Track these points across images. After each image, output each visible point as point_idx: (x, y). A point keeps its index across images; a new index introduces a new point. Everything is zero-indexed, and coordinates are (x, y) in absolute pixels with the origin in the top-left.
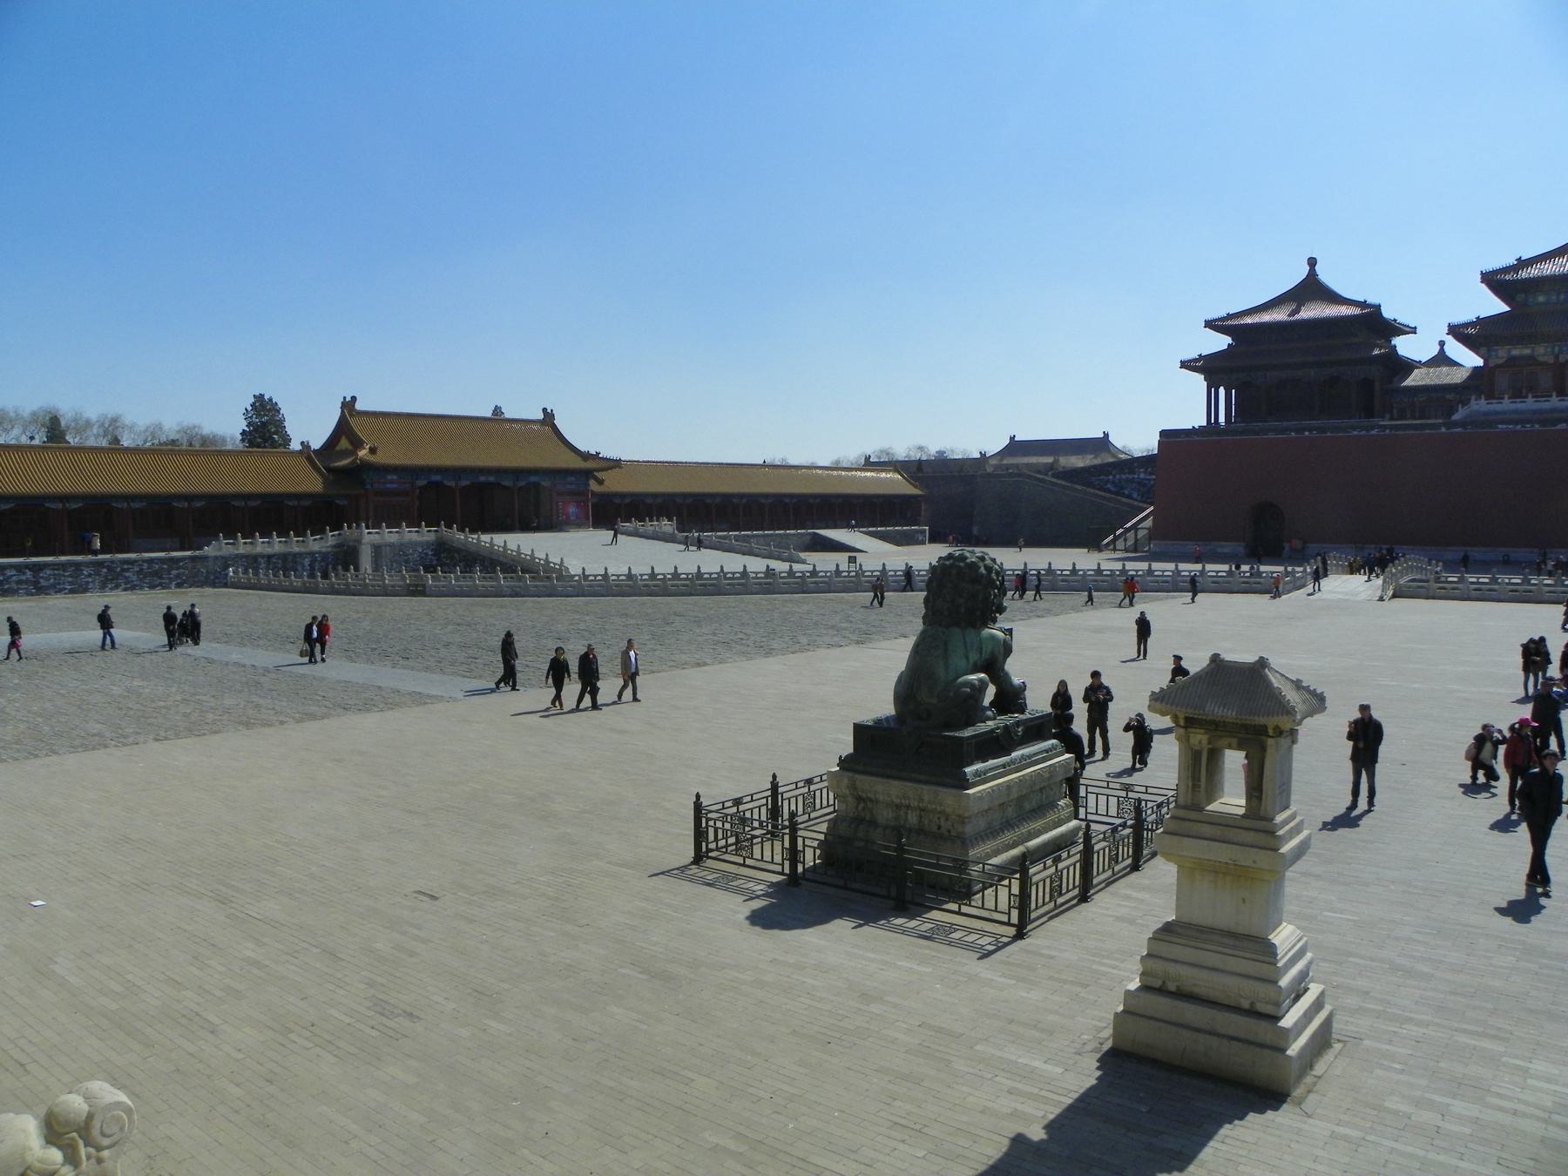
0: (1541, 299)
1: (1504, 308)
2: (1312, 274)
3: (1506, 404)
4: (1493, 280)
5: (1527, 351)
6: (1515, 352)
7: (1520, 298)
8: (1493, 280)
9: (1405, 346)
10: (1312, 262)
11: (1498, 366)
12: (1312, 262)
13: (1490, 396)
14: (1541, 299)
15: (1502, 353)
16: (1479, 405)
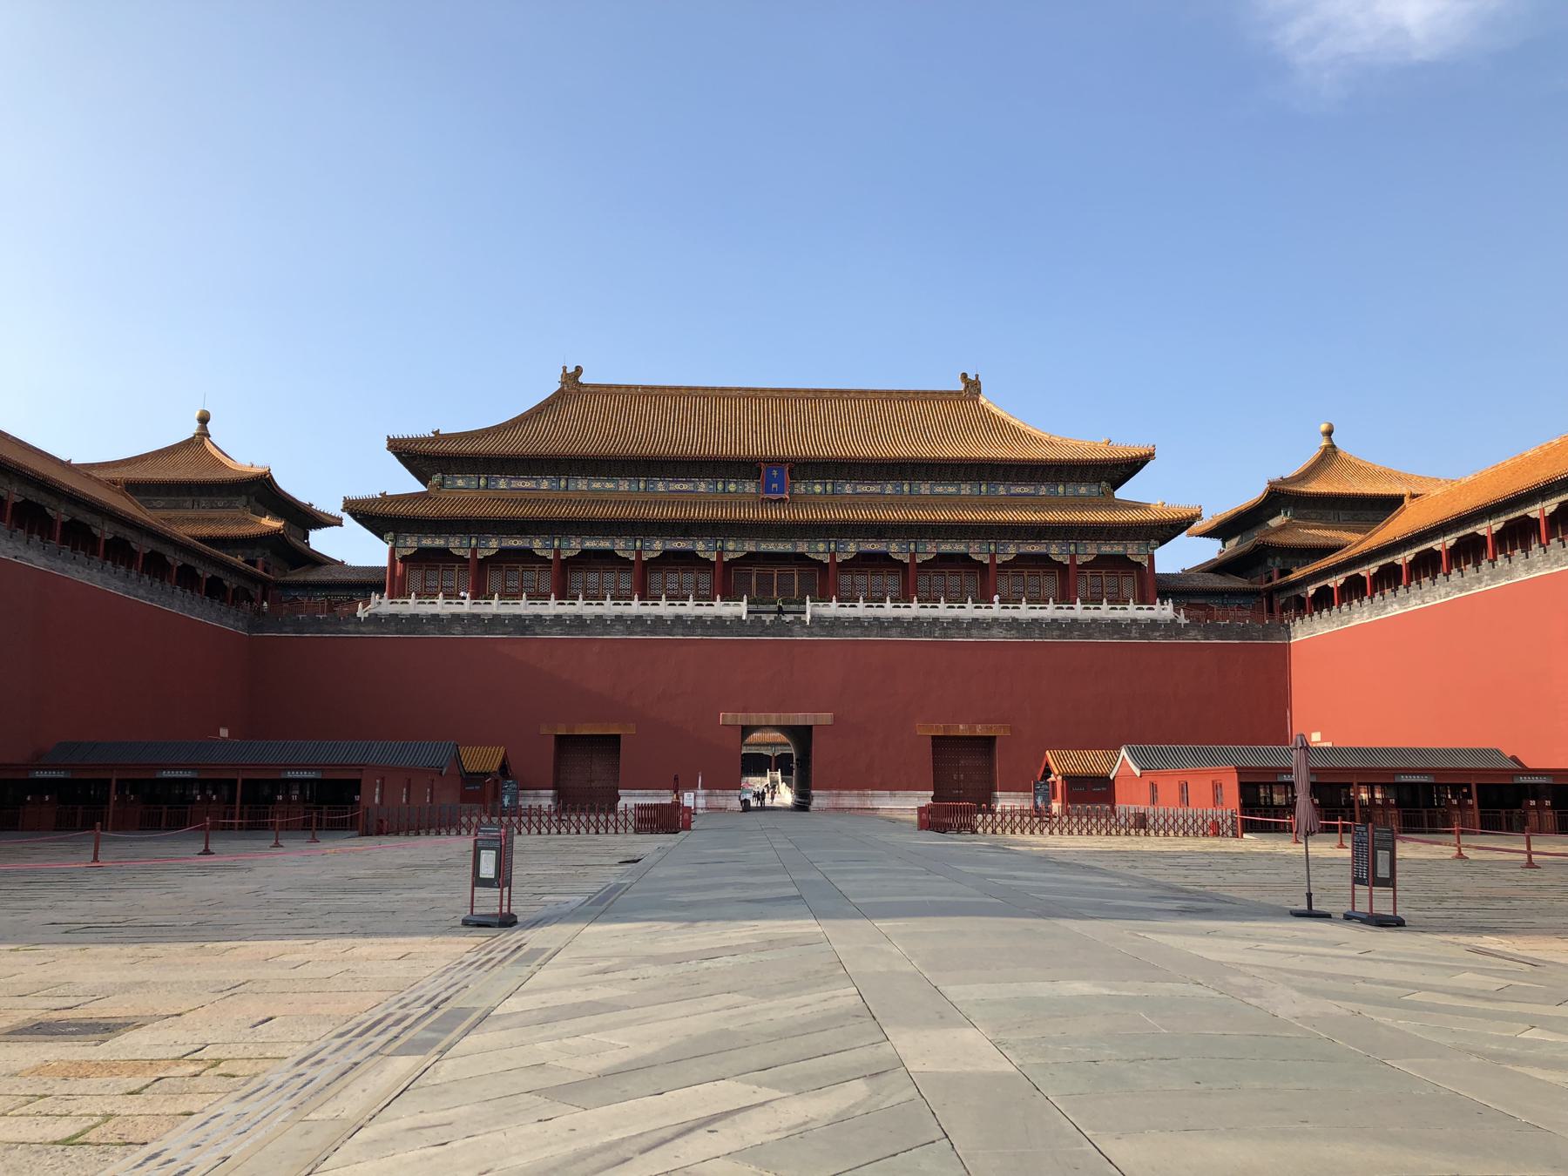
0: (460, 483)
1: (420, 488)
2: (204, 433)
3: (412, 606)
4: (409, 453)
5: (439, 542)
6: (427, 542)
7: (436, 478)
8: (409, 453)
9: (319, 541)
10: (204, 419)
11: (404, 559)
12: (204, 419)
13: (399, 592)
14: (460, 483)
15: (411, 543)
16: (381, 605)
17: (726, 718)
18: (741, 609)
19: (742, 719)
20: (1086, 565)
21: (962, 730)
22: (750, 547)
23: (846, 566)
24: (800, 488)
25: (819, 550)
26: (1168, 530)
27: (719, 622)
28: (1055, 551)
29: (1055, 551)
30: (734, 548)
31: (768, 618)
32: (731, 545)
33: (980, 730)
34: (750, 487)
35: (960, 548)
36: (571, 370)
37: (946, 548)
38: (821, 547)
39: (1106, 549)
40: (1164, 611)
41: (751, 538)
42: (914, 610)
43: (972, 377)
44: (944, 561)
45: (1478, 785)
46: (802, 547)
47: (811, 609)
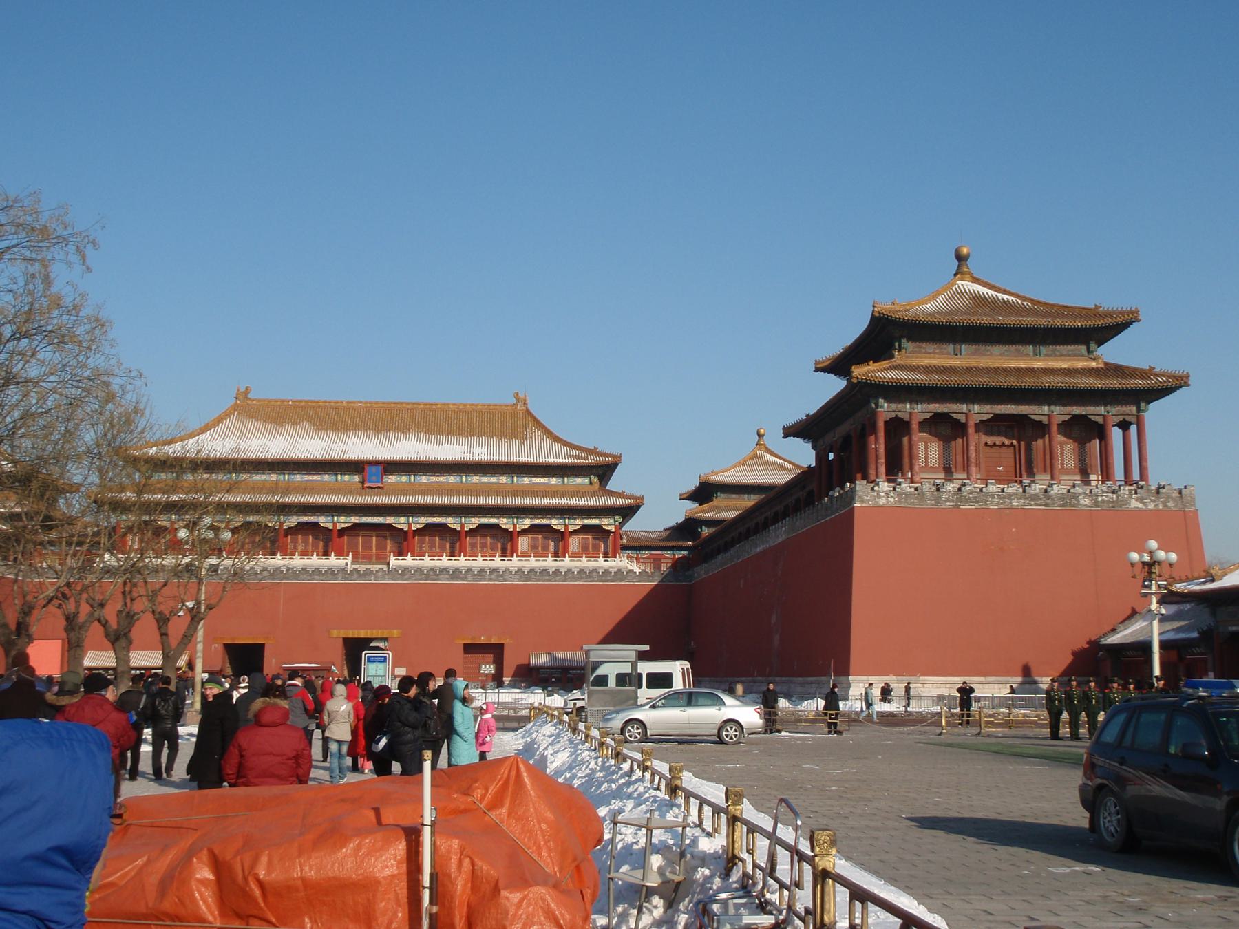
17: (335, 633)
18: (347, 562)
19: (344, 633)
20: (575, 532)
21: (483, 640)
22: (355, 520)
23: (419, 532)
24: (392, 479)
25: (400, 522)
26: (627, 512)
27: (330, 571)
28: (556, 523)
29: (556, 523)
30: (344, 522)
31: (362, 568)
32: (342, 519)
33: (493, 641)
34: (356, 478)
35: (494, 521)
36: (243, 389)
37: (484, 521)
38: (403, 520)
39: (588, 522)
40: (621, 562)
41: (356, 515)
42: (462, 562)
43: (521, 395)
44: (481, 526)
45: (648, 675)
46: (390, 520)
47: (393, 561)
